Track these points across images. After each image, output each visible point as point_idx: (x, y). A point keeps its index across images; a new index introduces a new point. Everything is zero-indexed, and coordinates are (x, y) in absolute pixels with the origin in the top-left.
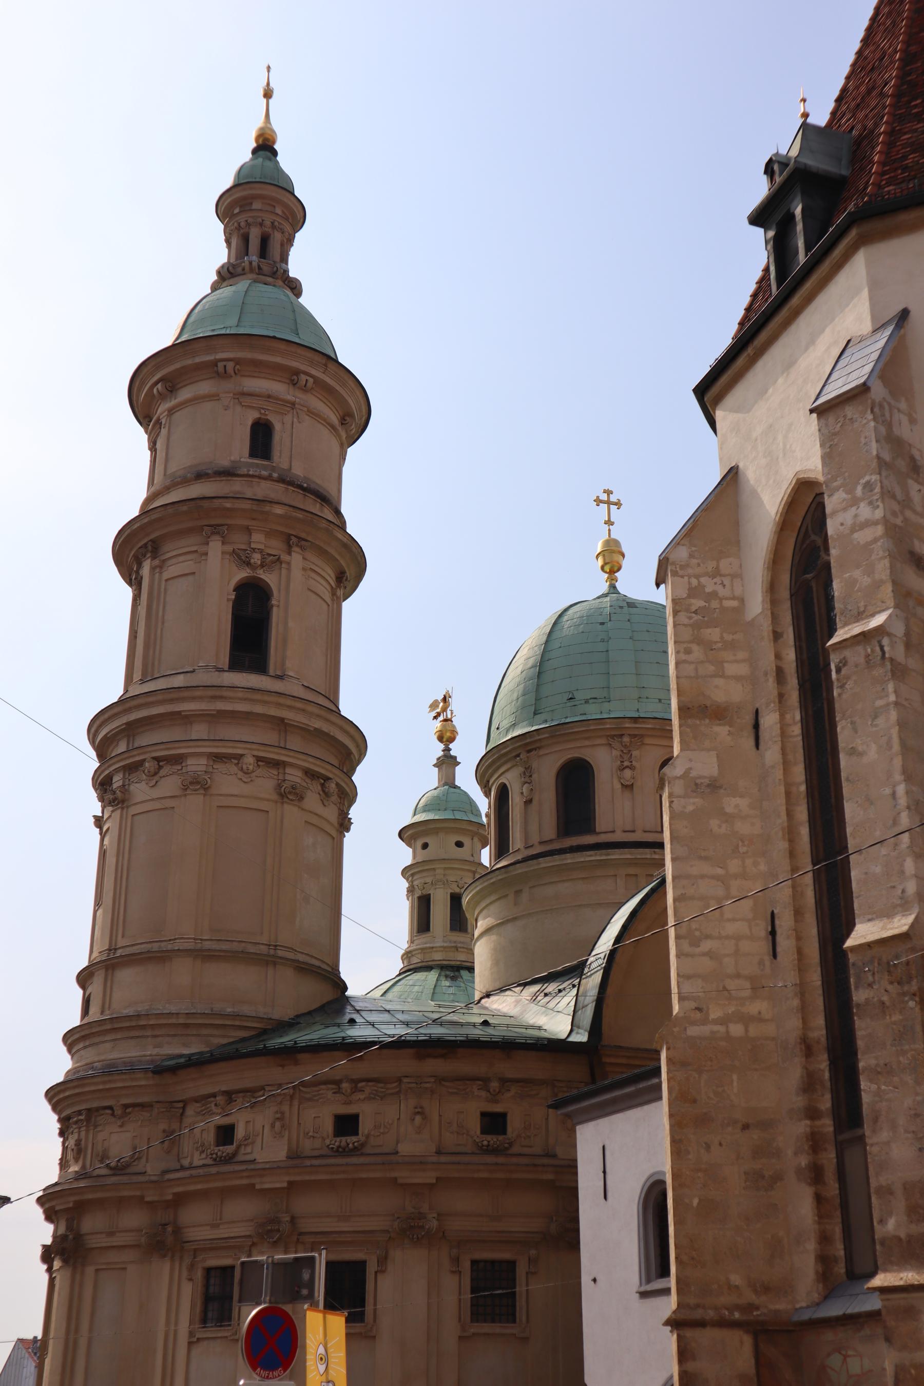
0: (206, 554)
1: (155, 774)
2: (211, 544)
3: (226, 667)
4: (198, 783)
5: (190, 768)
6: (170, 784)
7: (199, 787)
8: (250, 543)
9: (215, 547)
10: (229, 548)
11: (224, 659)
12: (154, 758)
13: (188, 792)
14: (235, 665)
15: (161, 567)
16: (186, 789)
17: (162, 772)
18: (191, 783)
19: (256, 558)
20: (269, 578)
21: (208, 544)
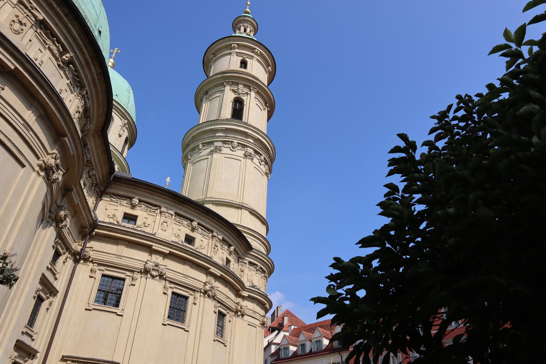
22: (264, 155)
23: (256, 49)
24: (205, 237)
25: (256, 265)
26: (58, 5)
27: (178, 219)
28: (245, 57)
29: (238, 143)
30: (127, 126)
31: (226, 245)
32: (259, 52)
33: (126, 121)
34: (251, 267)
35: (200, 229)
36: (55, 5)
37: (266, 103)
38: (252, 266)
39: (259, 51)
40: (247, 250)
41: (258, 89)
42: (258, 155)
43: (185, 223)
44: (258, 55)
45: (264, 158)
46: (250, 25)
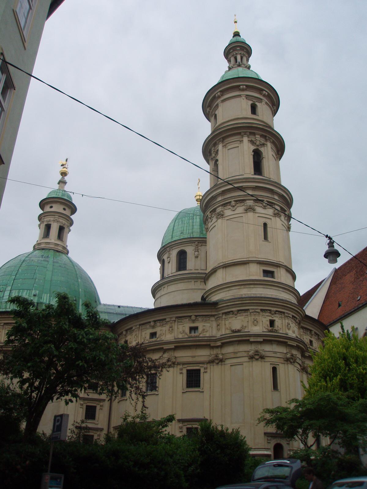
0: (243, 141)
1: (235, 205)
2: (244, 138)
3: (253, 174)
4: (251, 208)
5: (247, 204)
6: (240, 209)
7: (251, 210)
8: (255, 138)
9: (246, 139)
10: (250, 139)
11: (253, 173)
12: (235, 201)
13: (248, 211)
14: (255, 174)
15: (225, 146)
16: (247, 210)
17: (238, 205)
18: (249, 208)
19: (258, 143)
20: (262, 149)
21: (243, 138)
22: (232, 200)
23: (215, 95)
24: (164, 326)
25: (232, 311)
26: (3, 315)
27: (143, 327)
28: (214, 112)
29: (210, 212)
30: (200, 244)
31: (187, 318)
32: (219, 93)
33: (196, 243)
34: (228, 316)
35: (158, 324)
36: (3, 316)
37: (239, 134)
38: (229, 314)
39: (218, 92)
40: (215, 307)
41: (221, 137)
42: (228, 205)
43: (148, 326)
44: (222, 95)
45: (235, 201)
46: (234, 51)
